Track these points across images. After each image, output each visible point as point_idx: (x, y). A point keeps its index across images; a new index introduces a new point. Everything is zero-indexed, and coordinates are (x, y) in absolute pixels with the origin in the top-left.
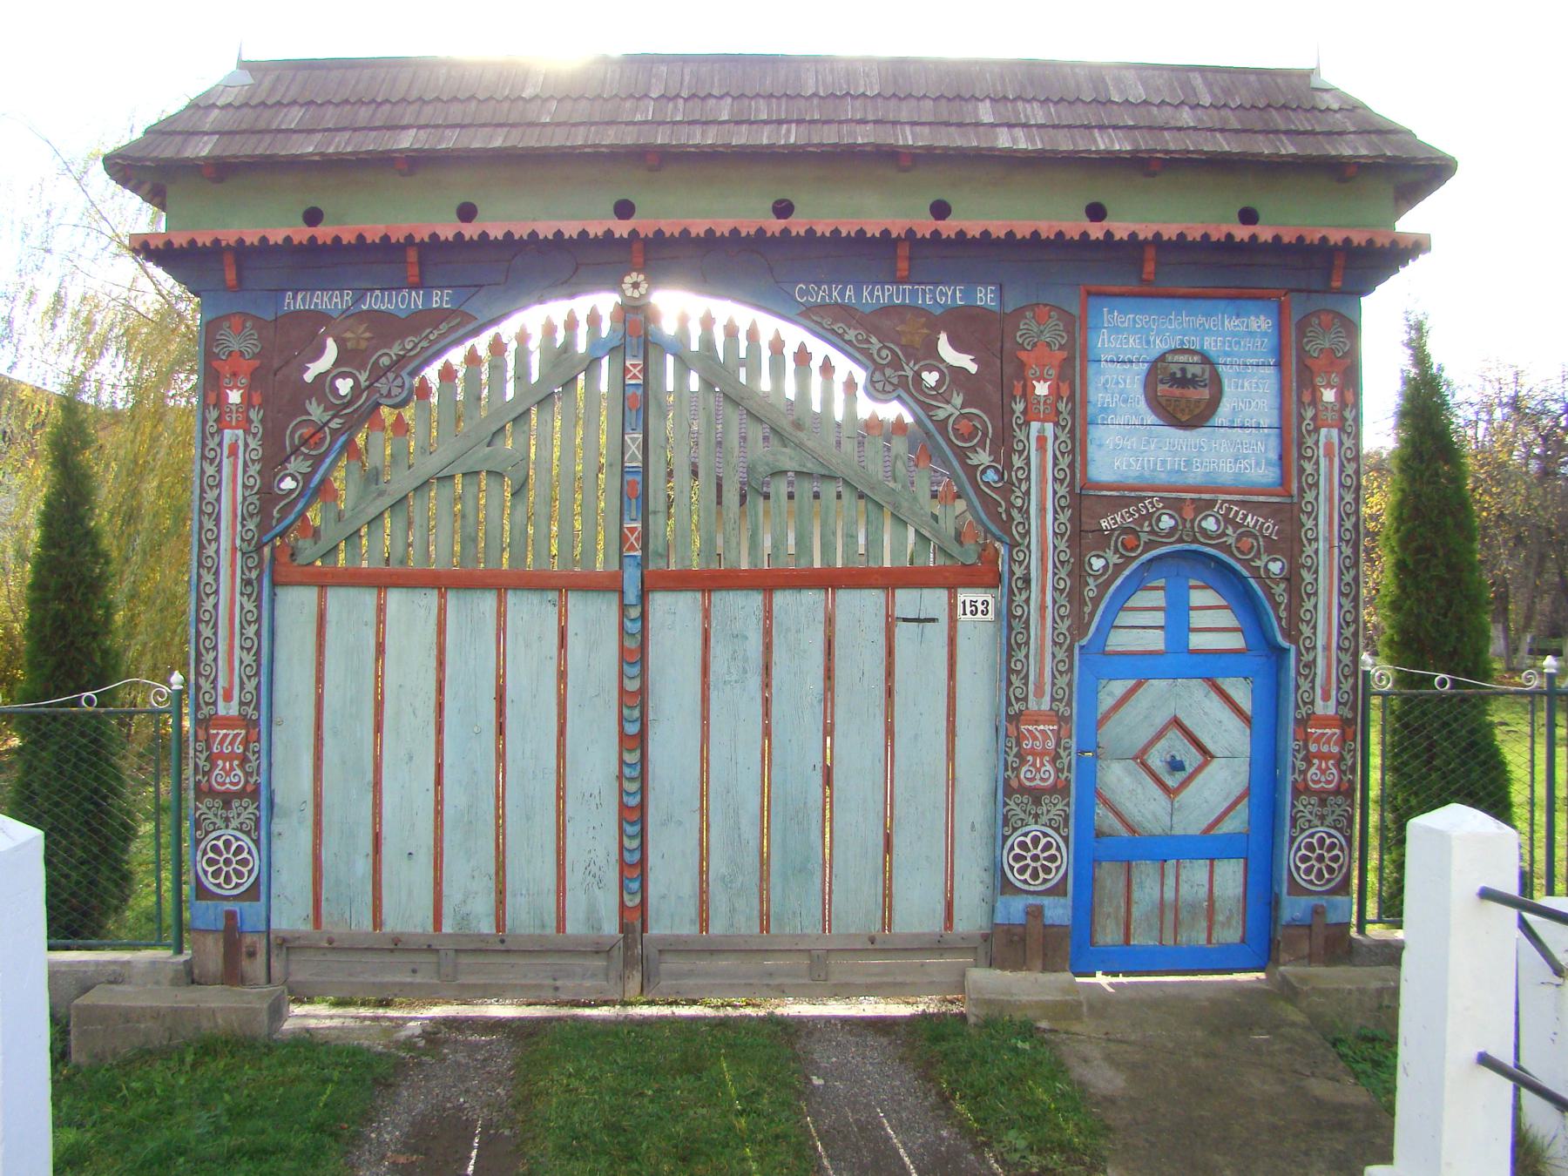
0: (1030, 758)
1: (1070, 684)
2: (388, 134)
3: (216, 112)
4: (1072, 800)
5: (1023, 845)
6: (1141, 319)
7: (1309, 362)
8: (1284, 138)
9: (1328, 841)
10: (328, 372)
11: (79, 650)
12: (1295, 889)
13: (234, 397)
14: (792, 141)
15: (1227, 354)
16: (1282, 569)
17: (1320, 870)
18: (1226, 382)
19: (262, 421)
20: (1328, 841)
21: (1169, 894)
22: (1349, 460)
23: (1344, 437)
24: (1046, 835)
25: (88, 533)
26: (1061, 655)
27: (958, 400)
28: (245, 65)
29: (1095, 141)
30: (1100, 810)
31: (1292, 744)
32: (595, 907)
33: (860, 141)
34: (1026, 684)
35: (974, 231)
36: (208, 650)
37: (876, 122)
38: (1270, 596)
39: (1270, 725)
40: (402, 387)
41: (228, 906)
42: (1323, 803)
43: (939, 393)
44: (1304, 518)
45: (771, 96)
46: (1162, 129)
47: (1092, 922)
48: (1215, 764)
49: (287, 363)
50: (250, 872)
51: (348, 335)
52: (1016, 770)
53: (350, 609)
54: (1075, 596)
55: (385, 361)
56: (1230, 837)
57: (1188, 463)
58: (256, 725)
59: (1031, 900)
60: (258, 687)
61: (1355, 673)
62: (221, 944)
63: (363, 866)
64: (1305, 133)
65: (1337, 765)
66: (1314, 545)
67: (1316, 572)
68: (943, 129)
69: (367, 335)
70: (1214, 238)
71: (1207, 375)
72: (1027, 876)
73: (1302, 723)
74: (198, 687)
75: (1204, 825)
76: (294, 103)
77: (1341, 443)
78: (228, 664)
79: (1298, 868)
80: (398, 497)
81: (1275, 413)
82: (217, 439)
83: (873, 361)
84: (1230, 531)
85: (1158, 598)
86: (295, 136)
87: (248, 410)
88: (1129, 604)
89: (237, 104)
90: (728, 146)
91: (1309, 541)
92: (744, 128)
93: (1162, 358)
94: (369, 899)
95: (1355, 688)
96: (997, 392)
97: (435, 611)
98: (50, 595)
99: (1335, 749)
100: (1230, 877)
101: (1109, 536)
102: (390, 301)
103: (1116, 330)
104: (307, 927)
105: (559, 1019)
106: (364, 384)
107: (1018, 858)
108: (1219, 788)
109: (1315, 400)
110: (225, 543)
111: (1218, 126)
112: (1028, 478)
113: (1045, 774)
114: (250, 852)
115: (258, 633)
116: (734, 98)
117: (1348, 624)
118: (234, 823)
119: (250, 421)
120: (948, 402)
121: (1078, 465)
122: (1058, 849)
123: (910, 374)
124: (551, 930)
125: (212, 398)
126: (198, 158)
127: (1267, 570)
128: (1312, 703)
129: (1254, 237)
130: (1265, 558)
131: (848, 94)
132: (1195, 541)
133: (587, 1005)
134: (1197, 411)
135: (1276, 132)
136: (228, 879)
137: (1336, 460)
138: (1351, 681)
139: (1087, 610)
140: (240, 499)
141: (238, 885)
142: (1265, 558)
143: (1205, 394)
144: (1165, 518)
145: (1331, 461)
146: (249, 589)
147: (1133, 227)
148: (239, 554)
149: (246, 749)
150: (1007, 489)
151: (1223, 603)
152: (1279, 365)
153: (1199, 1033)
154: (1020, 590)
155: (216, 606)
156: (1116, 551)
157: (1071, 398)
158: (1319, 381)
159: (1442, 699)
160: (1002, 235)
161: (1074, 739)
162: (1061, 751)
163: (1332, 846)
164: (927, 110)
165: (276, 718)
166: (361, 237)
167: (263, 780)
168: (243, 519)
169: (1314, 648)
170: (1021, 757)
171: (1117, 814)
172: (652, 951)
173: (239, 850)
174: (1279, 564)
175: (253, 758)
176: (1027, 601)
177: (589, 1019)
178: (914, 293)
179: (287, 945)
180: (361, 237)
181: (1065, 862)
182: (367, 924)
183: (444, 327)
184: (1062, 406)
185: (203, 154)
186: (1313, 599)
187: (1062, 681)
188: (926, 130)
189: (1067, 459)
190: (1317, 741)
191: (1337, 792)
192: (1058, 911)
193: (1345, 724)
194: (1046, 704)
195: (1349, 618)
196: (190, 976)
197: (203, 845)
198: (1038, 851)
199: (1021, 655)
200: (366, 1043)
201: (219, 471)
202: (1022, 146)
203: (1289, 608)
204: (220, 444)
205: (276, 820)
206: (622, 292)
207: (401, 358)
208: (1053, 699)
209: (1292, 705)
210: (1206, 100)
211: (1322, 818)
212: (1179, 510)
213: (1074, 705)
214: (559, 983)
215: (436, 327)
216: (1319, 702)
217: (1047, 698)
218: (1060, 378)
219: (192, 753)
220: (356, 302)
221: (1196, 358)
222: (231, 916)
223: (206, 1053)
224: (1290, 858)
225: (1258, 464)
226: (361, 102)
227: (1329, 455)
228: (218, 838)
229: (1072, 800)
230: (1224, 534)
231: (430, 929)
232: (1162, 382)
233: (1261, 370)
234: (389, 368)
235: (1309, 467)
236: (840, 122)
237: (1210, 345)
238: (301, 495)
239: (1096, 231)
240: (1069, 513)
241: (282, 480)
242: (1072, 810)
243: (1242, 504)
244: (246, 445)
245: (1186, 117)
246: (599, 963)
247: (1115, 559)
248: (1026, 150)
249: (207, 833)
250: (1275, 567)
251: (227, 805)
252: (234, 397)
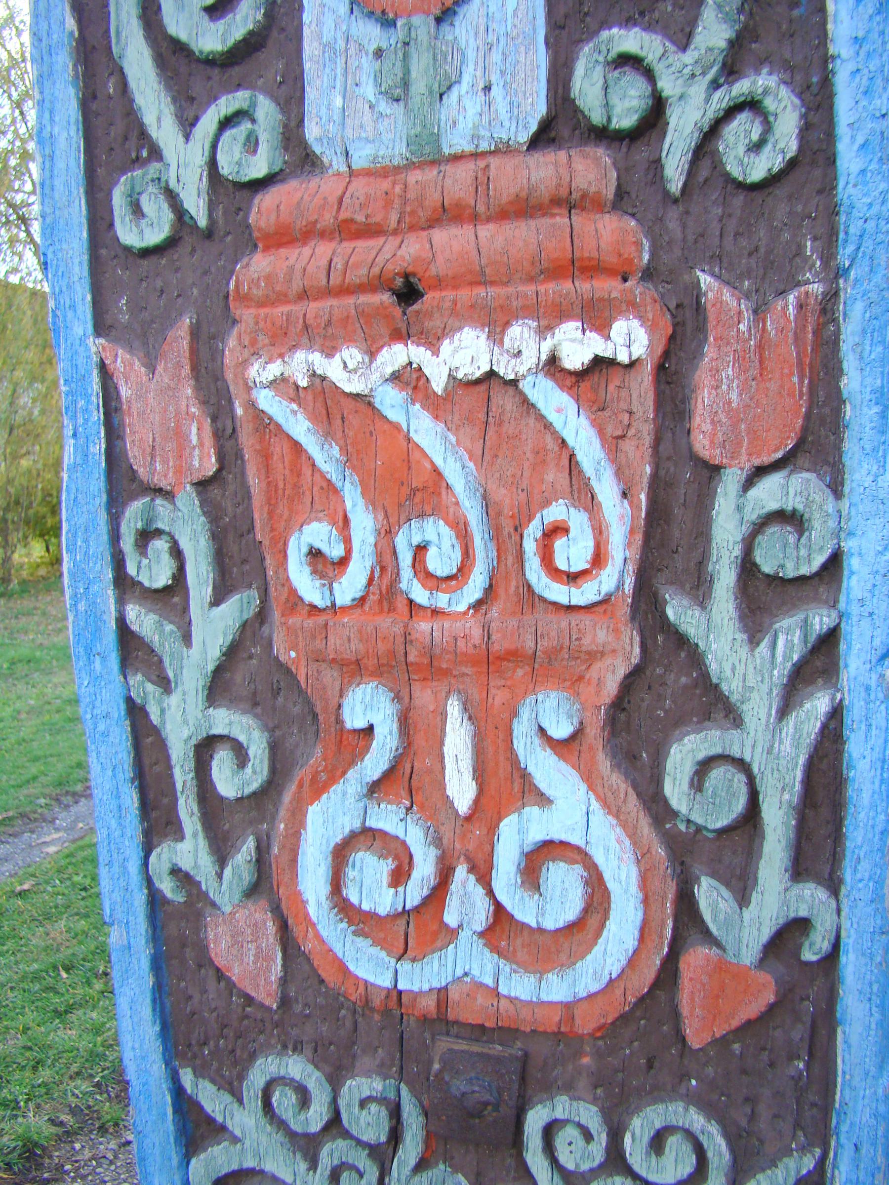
0: (367, 706)
52: (251, 824)
162: (713, 626)
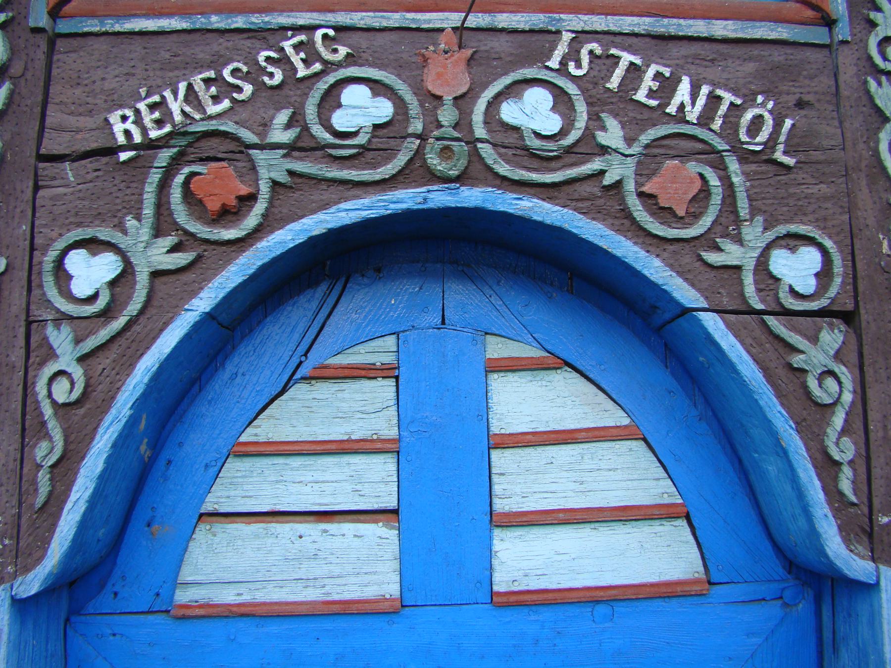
16: (824, 275)
38: (789, 380)
84: (612, 134)
85: (367, 407)
88: (264, 430)
101: (138, 167)
127: (767, 280)
130: (755, 234)
132: (475, 172)
139: (46, 453)
142: (755, 234)
151: (616, 418)
174: (810, 258)
212: (414, 69)
247: (160, 255)
250: (797, 269)
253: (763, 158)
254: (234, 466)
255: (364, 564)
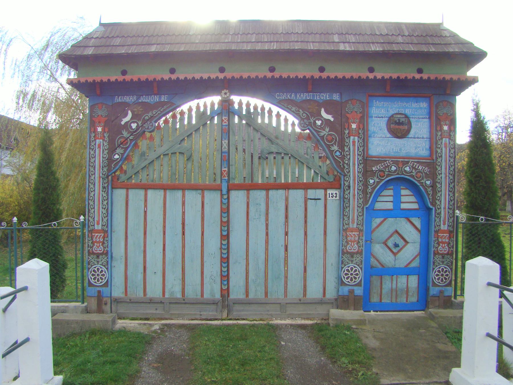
0: (350, 243)
1: (363, 219)
2: (148, 47)
3: (93, 40)
4: (363, 256)
5: (348, 270)
6: (386, 104)
7: (439, 117)
8: (431, 46)
9: (445, 270)
10: (129, 121)
11: (50, 209)
12: (434, 285)
13: (100, 129)
14: (275, 48)
15: (413, 115)
17: (442, 279)
18: (413, 124)
19: (108, 137)
20: (445, 270)
21: (394, 286)
22: (452, 148)
23: (451, 141)
24: (355, 267)
25: (52, 172)
26: (360, 210)
27: (327, 130)
28: (101, 24)
29: (371, 48)
30: (372, 259)
31: (433, 239)
32: (213, 290)
33: (296, 48)
34: (349, 219)
35: (332, 76)
36: (92, 209)
37: (301, 42)
39: (426, 232)
40: (152, 126)
41: (98, 289)
42: (443, 257)
43: (322, 128)
44: (437, 167)
45: (268, 33)
46: (392, 43)
47: (370, 295)
48: (409, 245)
49: (116, 119)
50: (105, 278)
51: (135, 110)
52: (346, 246)
53: (137, 195)
54: (365, 192)
55: (147, 118)
56: (414, 268)
57: (400, 149)
58: (107, 232)
59: (350, 288)
60: (107, 220)
61: (454, 216)
62: (96, 301)
63: (140, 276)
64: (438, 44)
65: (448, 246)
66: (441, 176)
67: (441, 184)
68: (323, 44)
69: (141, 110)
70: (409, 78)
71: (406, 122)
72: (349, 280)
73: (436, 232)
74: (89, 220)
75: (405, 264)
76: (118, 37)
77: (449, 143)
78: (97, 213)
79: (435, 278)
80: (151, 160)
81: (428, 134)
82: (94, 143)
83: (301, 117)
84: (414, 171)
85: (391, 192)
86: (118, 47)
87: (104, 134)
88: (382, 194)
89: (100, 37)
90: (255, 50)
91: (439, 174)
92: (260, 44)
93: (392, 116)
94: (142, 286)
95: (453, 221)
96: (339, 127)
97: (163, 197)
98: (40, 192)
99: (447, 240)
100: (413, 281)
101: (375, 173)
102: (148, 99)
103: (378, 107)
104: (123, 295)
105: (202, 324)
106: (140, 125)
107: (346, 274)
108: (410, 252)
109: (441, 129)
110: (97, 175)
111: (410, 42)
112: (350, 154)
113: (354, 248)
114: (105, 272)
115: (107, 203)
116: (256, 34)
117: (451, 200)
118: (100, 263)
119: (104, 137)
120: (324, 130)
121: (365, 150)
122: (359, 271)
123: (312, 121)
124: (199, 297)
125: (93, 130)
126: (89, 55)
127: (426, 183)
128: (440, 226)
129: (421, 78)
130: (425, 180)
131: (292, 33)
132: (403, 174)
133: (211, 320)
134: (403, 133)
135: (429, 44)
136: (98, 280)
137: (448, 148)
138: (452, 219)
139: (368, 196)
140: (101, 161)
141: (101, 282)
142: (425, 180)
143: (406, 127)
144: (393, 167)
145: (446, 149)
146: (104, 190)
147: (383, 75)
148: (101, 179)
149: (104, 240)
150: (343, 158)
151: (412, 194)
152: (430, 118)
153: (403, 330)
154: (347, 190)
155: (94, 195)
156: (377, 177)
157: (363, 129)
158: (442, 123)
159: (483, 225)
160: (341, 78)
161: (364, 237)
162: (360, 240)
163: (446, 271)
164: (318, 38)
165: (113, 230)
166: (139, 79)
167: (109, 249)
168: (103, 167)
169: (441, 208)
170: (347, 242)
171: (378, 260)
172: (231, 303)
173: (102, 271)
174: (429, 182)
175: (106, 242)
176: (349, 193)
177: (211, 325)
178: (313, 96)
179: (117, 301)
180: (139, 79)
181: (361, 276)
182: (142, 294)
183: (165, 107)
184: (360, 131)
185: (90, 53)
186: (440, 193)
187: (360, 218)
188: (317, 44)
189: (362, 148)
190: (441, 238)
191: (448, 254)
192: (359, 291)
193: (450, 232)
194: (355, 226)
195: (452, 199)
196: (87, 311)
197: (90, 270)
198: (352, 272)
199: (347, 210)
200: (142, 331)
201: (95, 152)
202: (348, 49)
203: (432, 195)
204: (95, 144)
205: (113, 262)
206: (221, 96)
207: (152, 117)
208: (357, 224)
209: (433, 226)
210: (407, 34)
211: (443, 262)
212: (398, 164)
213: (364, 226)
214: (201, 313)
215: (163, 107)
216: (442, 225)
217: (355, 224)
218: (360, 122)
219: (87, 241)
220: (138, 99)
221: (403, 116)
222: (99, 292)
223: (93, 334)
224: (432, 275)
225: (423, 150)
226: (139, 36)
227: (446, 147)
228: (95, 268)
229: (363, 256)
230: (412, 172)
231: (161, 296)
232: (392, 123)
233: (424, 120)
234: (148, 120)
235: (439, 151)
236: (290, 42)
237: (408, 112)
238: (121, 160)
239: (371, 76)
240: (362, 165)
241: (115, 155)
242: (363, 259)
243: (418, 162)
244: (103, 144)
245: (400, 39)
246: (214, 307)
247: (377, 180)
248: (349, 51)
249: (92, 266)
250: (428, 183)
251: (98, 257)
252: (100, 129)
253: (426, 173)
254: (379, 197)
255: (390, 206)
